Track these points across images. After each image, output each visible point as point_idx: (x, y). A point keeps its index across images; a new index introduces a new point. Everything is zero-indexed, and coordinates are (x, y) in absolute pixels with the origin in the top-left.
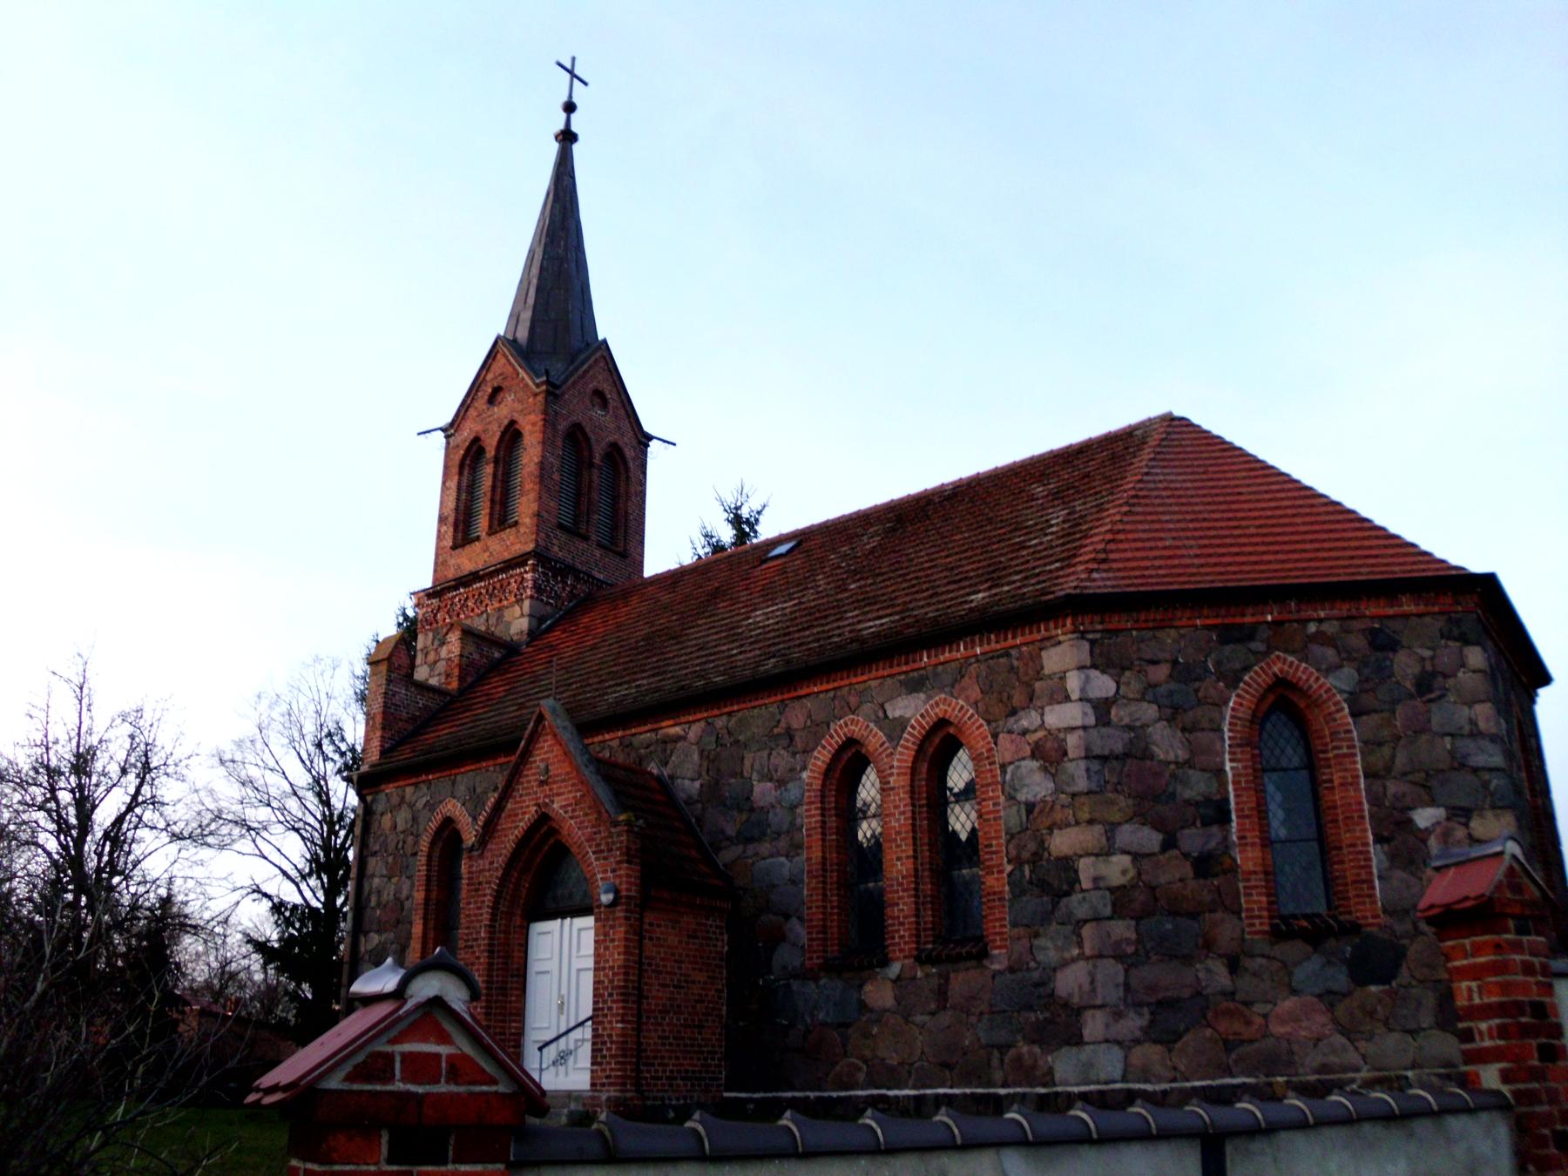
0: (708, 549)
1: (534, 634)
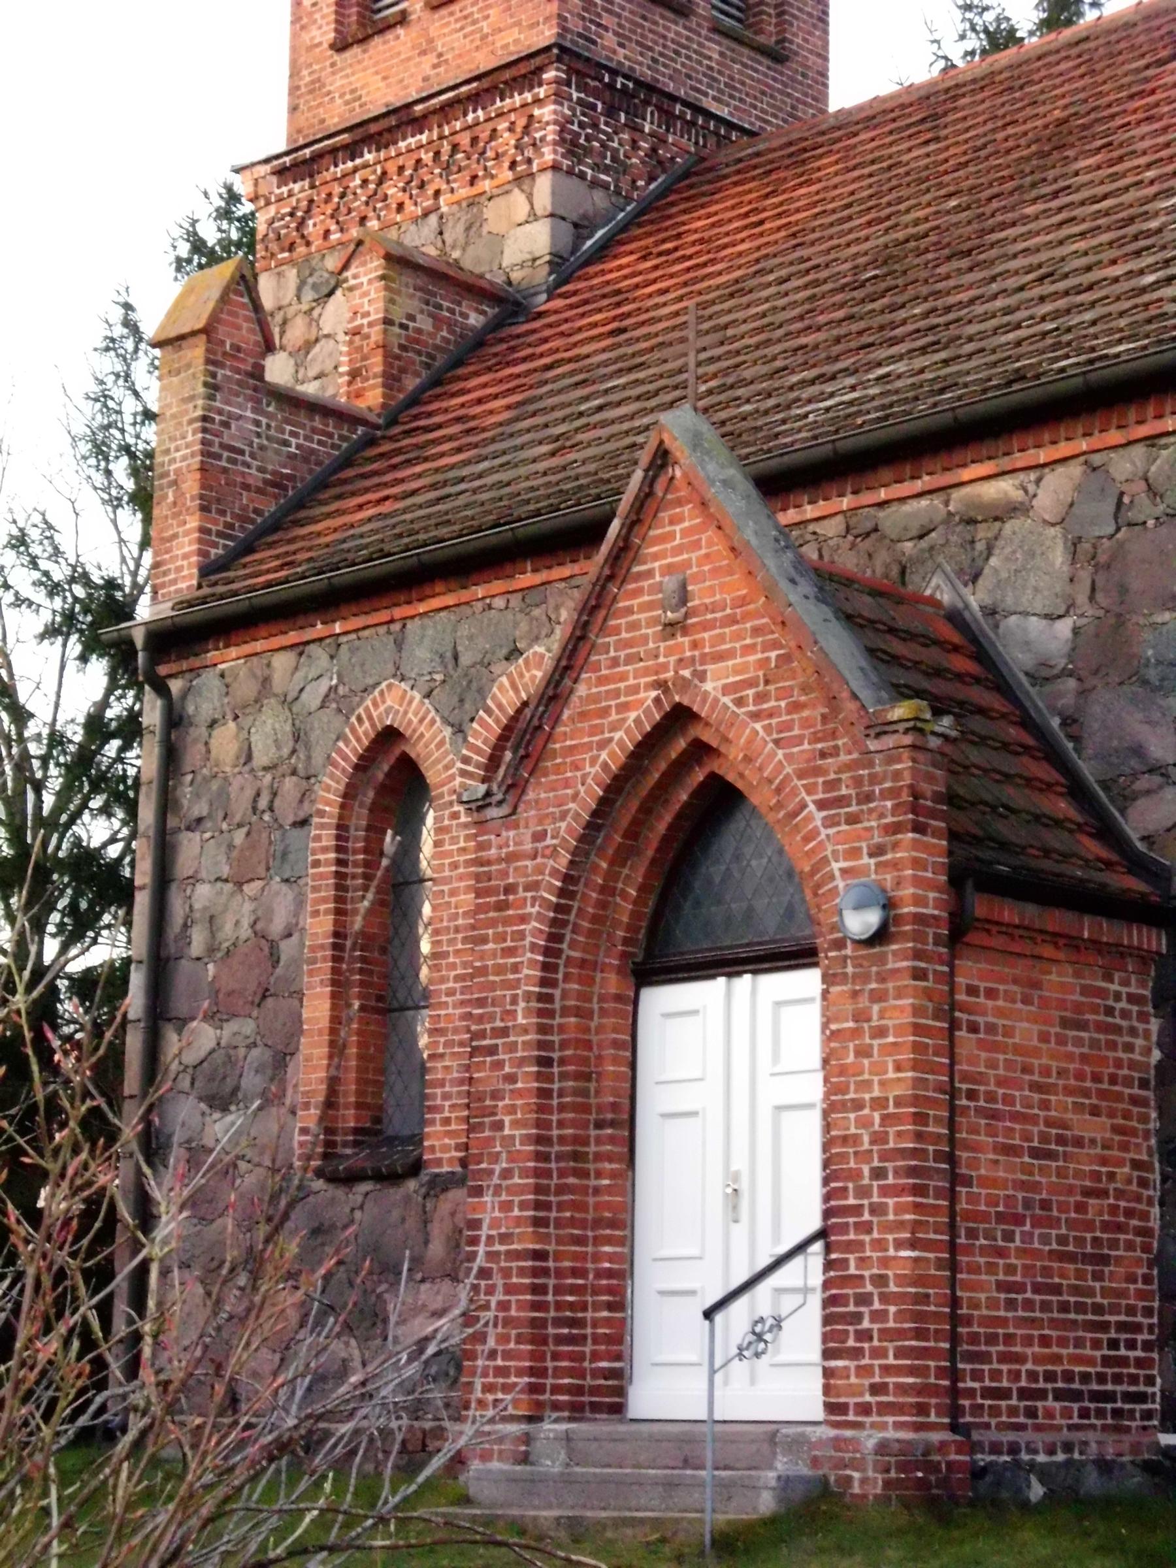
0: (974, 43)
1: (565, 267)
